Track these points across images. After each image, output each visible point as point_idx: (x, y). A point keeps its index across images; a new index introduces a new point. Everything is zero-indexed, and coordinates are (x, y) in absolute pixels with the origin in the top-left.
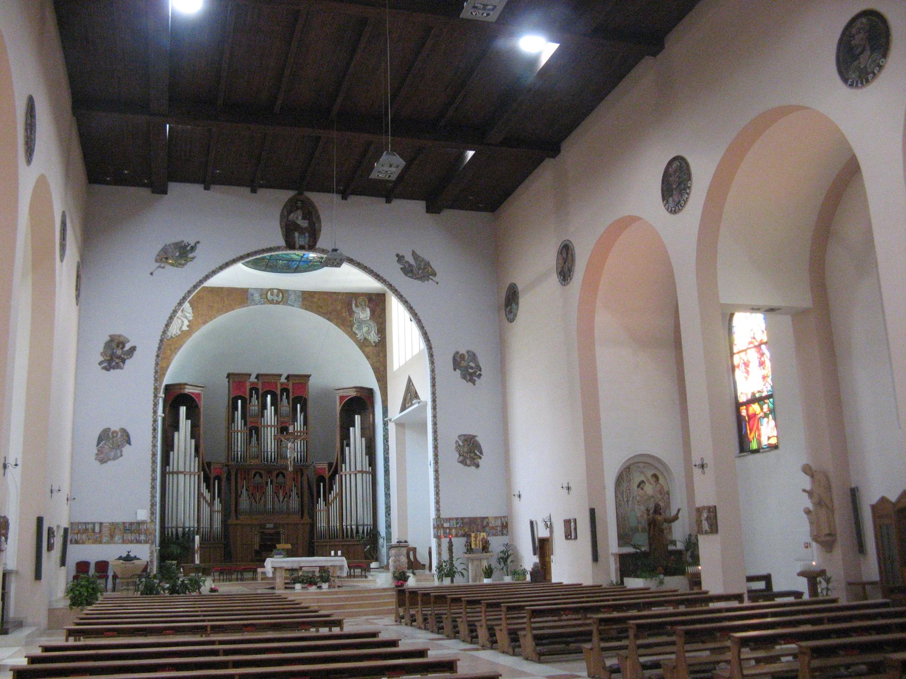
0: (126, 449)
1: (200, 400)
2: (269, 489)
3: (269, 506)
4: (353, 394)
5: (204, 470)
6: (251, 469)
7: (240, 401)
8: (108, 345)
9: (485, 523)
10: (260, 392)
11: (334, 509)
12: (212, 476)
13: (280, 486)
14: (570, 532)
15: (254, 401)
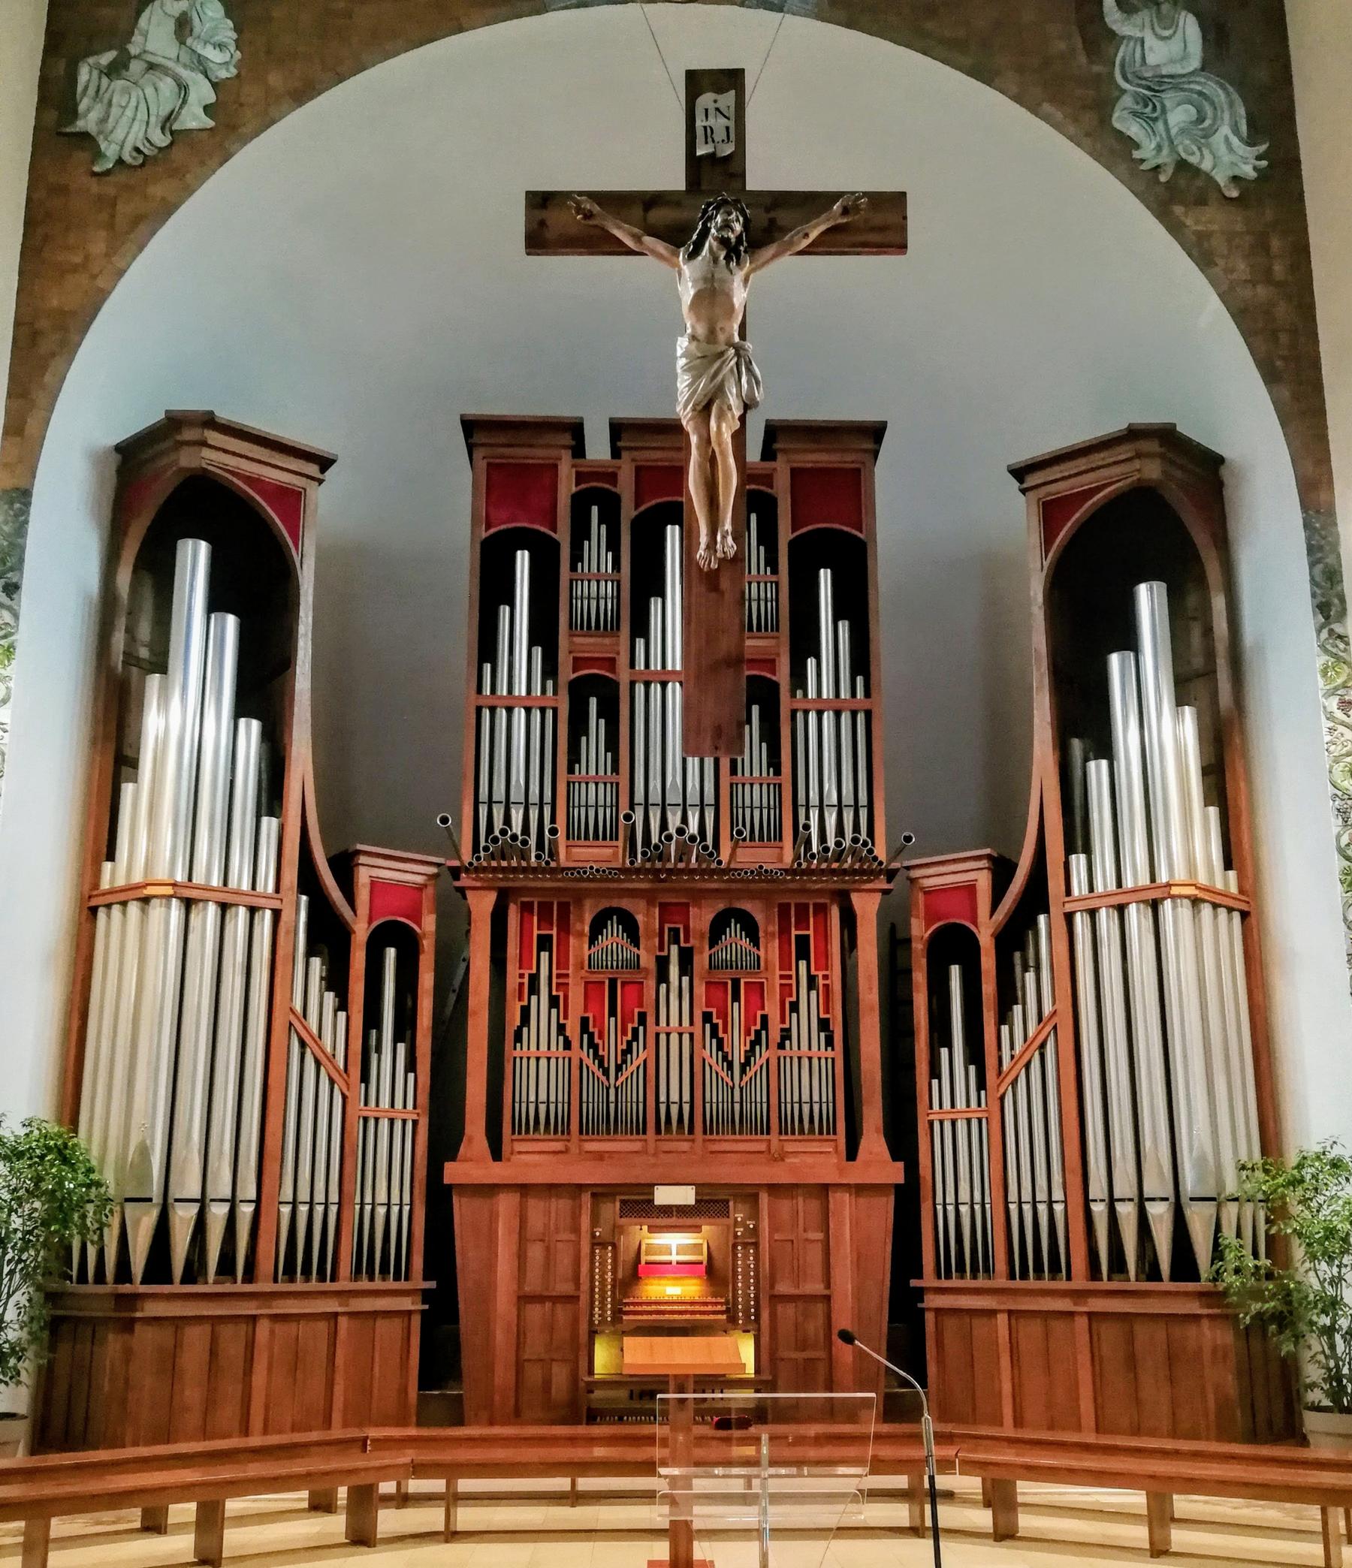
2: (675, 1007)
3: (675, 1090)
5: (308, 880)
6: (579, 897)
7: (523, 560)
10: (628, 512)
13: (728, 986)
15: (597, 554)
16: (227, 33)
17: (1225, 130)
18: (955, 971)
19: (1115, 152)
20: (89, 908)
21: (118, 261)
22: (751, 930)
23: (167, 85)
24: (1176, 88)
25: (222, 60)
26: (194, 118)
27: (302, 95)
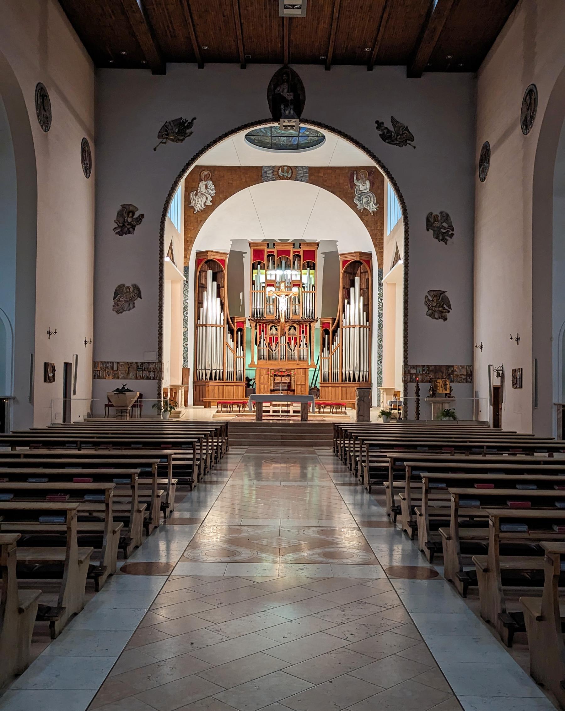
0: (138, 302)
1: (223, 264)
3: (283, 354)
4: (354, 258)
5: (228, 323)
8: (120, 214)
9: (450, 371)
11: (336, 356)
12: (235, 329)
14: (517, 383)
16: (213, 188)
17: (372, 202)
18: (326, 336)
19: (354, 207)
20: (196, 327)
21: (199, 228)
22: (295, 329)
23: (204, 197)
24: (365, 195)
25: (213, 192)
26: (209, 203)
27: (226, 198)
